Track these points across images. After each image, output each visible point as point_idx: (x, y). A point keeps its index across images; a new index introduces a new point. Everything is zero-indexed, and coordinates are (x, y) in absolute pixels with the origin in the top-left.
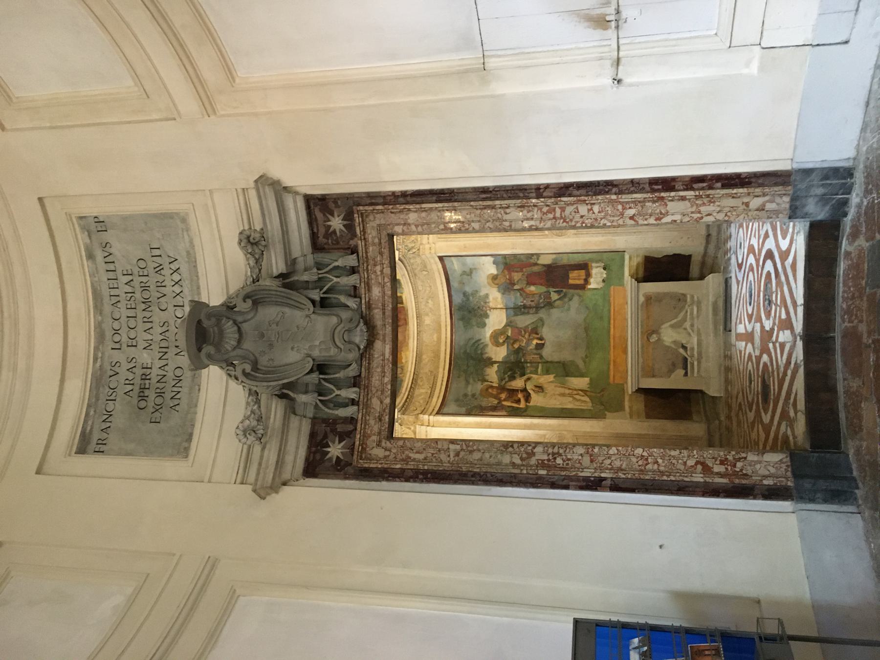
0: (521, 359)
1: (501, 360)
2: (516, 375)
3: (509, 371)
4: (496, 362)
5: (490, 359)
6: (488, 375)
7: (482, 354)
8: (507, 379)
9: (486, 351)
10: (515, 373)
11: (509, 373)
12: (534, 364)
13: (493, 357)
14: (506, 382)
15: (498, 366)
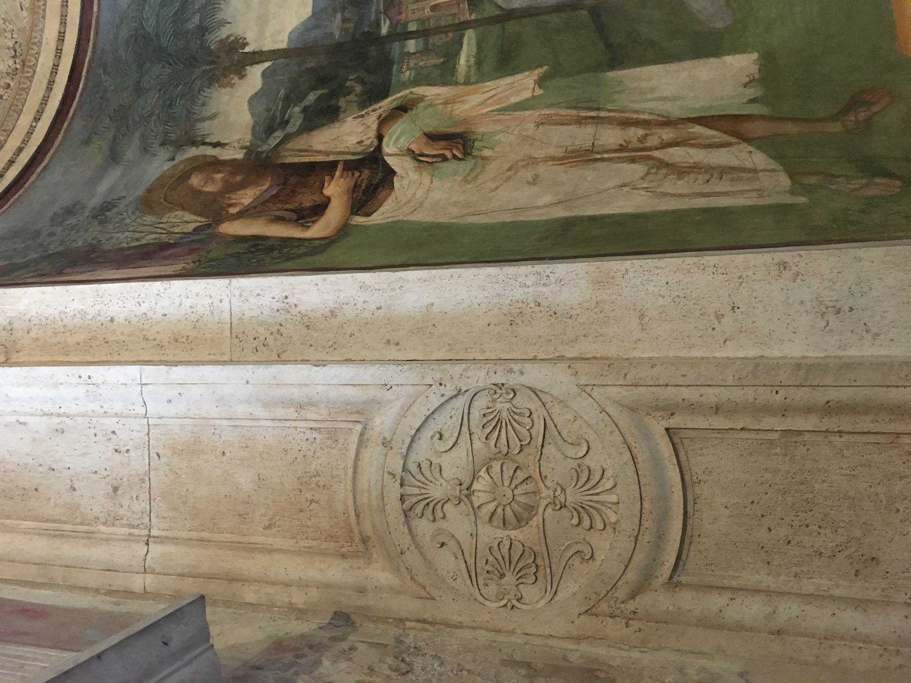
0: (378, 26)
1: (283, 45)
2: (342, 102)
3: (312, 88)
4: (258, 57)
5: (235, 45)
6: (214, 117)
7: (203, 30)
8: (296, 123)
9: (220, 16)
10: (340, 91)
11: (312, 97)
12: (436, 40)
13: (250, 36)
14: (287, 138)
15: (264, 74)
